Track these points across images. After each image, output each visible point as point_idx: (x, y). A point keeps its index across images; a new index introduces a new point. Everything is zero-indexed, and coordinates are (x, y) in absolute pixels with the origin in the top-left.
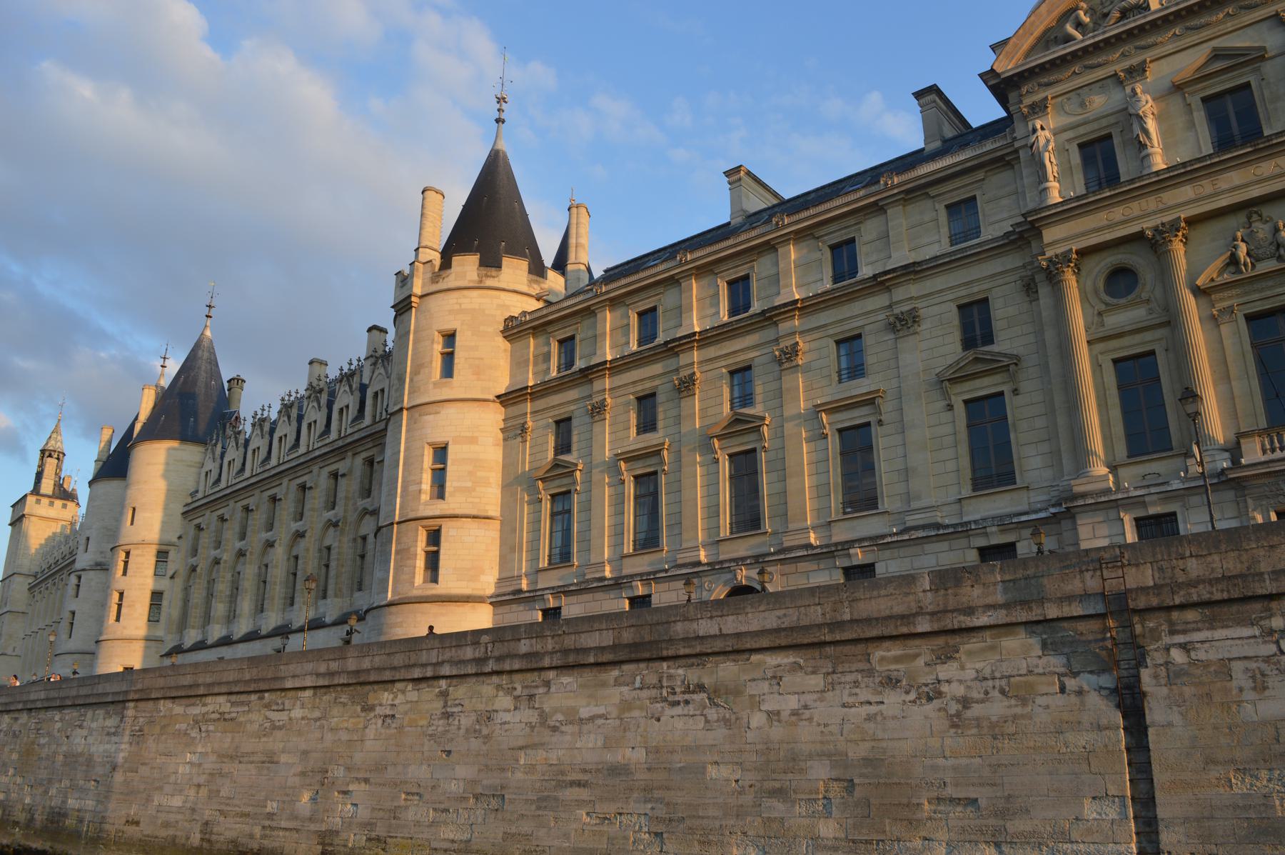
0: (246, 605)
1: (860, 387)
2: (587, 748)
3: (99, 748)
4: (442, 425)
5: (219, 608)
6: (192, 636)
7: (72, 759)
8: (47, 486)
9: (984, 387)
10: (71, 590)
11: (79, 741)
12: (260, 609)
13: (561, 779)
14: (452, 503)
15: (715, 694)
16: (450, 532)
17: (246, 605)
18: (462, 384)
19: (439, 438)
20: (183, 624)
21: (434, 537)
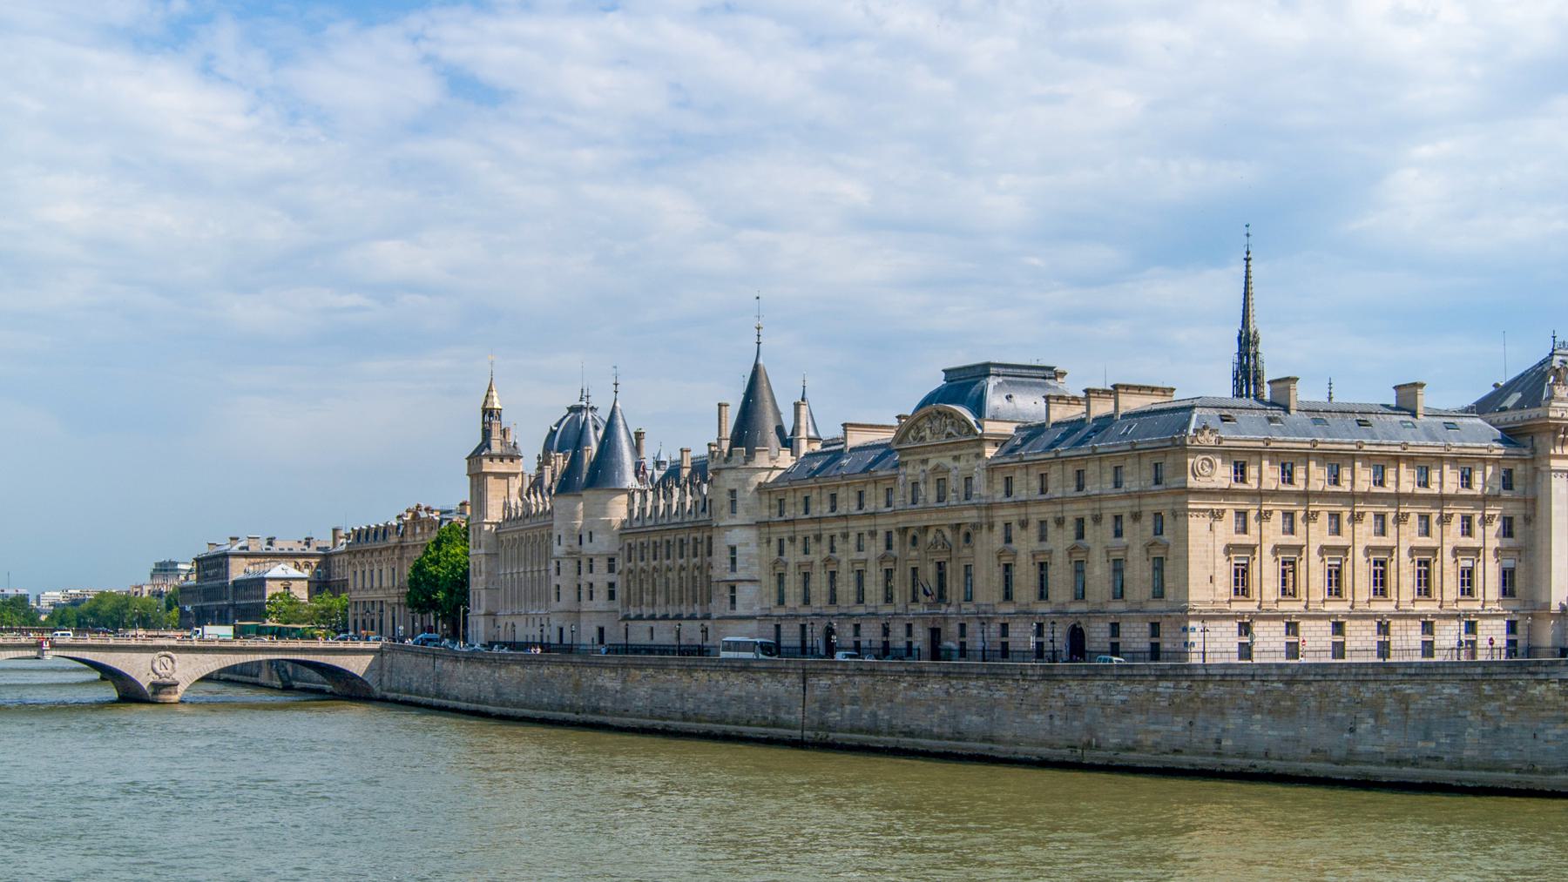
0: (660, 599)
1: (863, 555)
2: (735, 691)
3: (609, 685)
4: (737, 537)
5: (647, 598)
6: (633, 612)
7: (598, 688)
8: (496, 447)
9: (889, 565)
10: (553, 572)
11: (599, 681)
12: (667, 602)
13: (733, 698)
14: (740, 574)
15: (757, 681)
16: (739, 587)
17: (660, 599)
18: (741, 517)
19: (732, 543)
20: (628, 602)
21: (733, 589)
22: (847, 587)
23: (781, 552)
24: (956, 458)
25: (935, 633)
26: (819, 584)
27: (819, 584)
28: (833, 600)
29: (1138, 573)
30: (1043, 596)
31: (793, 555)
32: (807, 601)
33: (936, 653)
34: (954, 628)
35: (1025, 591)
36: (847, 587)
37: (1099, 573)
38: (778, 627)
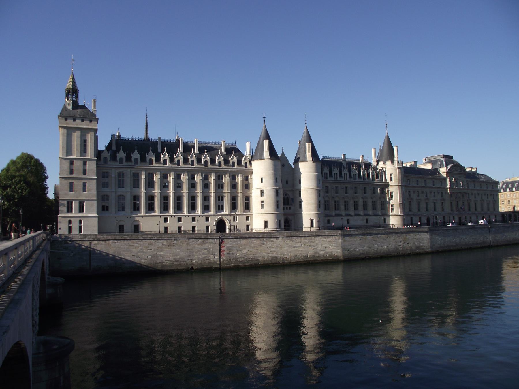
22: (431, 206)
23: (410, 195)
24: (460, 177)
25: (460, 218)
26: (423, 205)
27: (423, 205)
28: (435, 209)
29: (491, 206)
30: (476, 210)
31: (414, 196)
32: (419, 210)
33: (428, 224)
34: (464, 217)
35: (473, 209)
36: (431, 206)
37: (485, 205)
38: (411, 218)
